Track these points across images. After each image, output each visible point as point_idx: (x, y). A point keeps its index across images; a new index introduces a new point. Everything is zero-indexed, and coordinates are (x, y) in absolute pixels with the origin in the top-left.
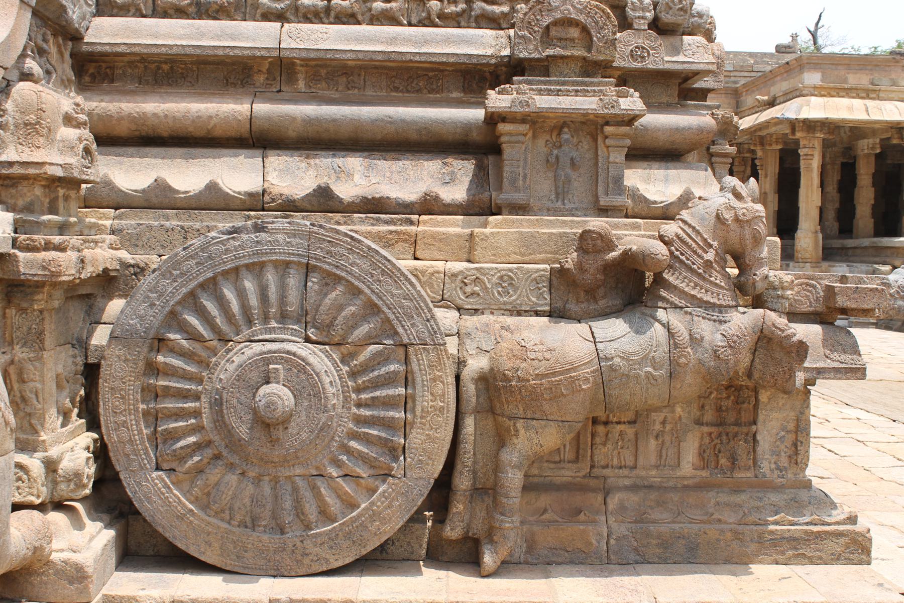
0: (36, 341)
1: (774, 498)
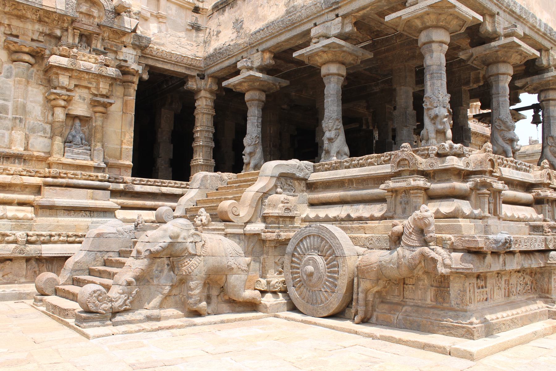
0: (267, 253)
1: (450, 313)
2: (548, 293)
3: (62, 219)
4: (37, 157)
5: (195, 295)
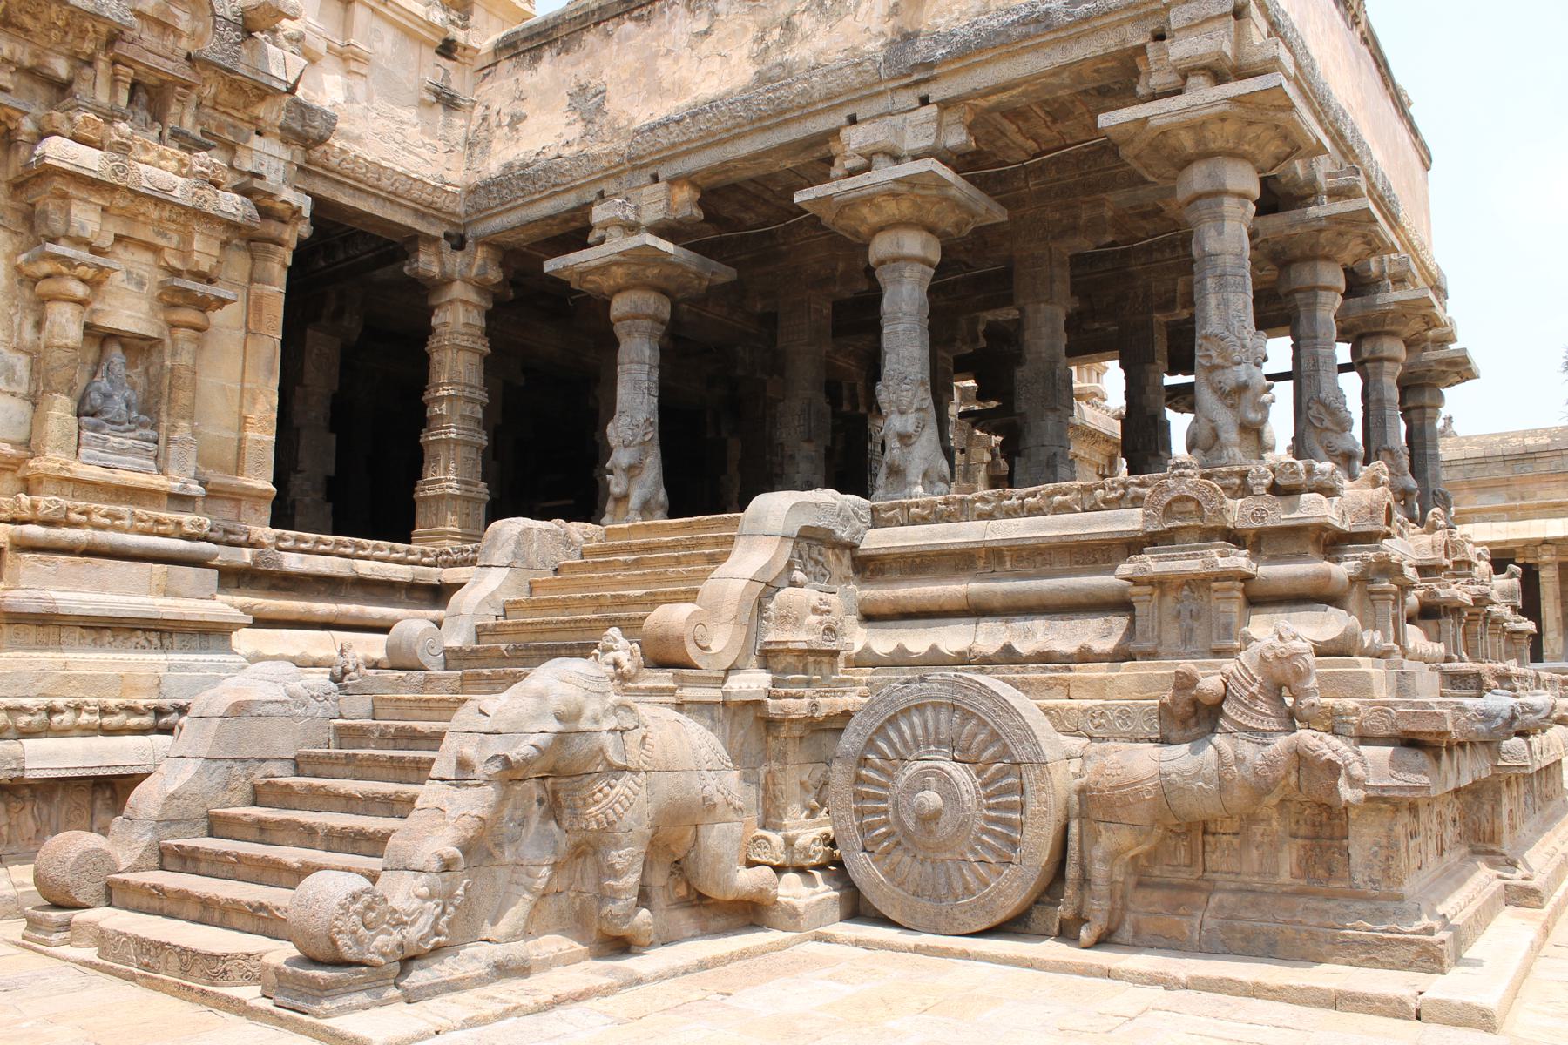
0: (782, 757)
2: (1492, 840)
3: (80, 655)
5: (626, 890)
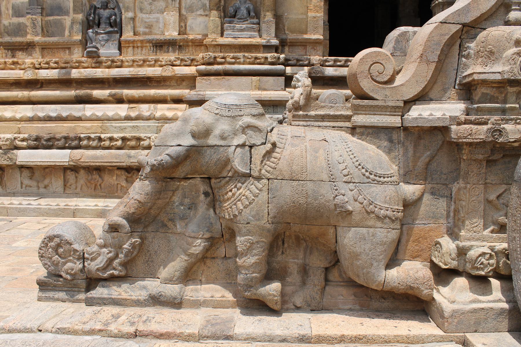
4: (193, 41)
5: (244, 267)
